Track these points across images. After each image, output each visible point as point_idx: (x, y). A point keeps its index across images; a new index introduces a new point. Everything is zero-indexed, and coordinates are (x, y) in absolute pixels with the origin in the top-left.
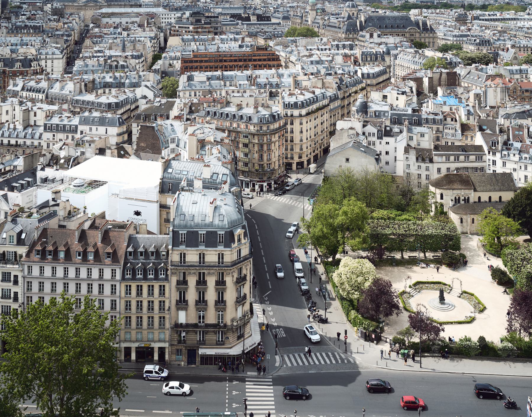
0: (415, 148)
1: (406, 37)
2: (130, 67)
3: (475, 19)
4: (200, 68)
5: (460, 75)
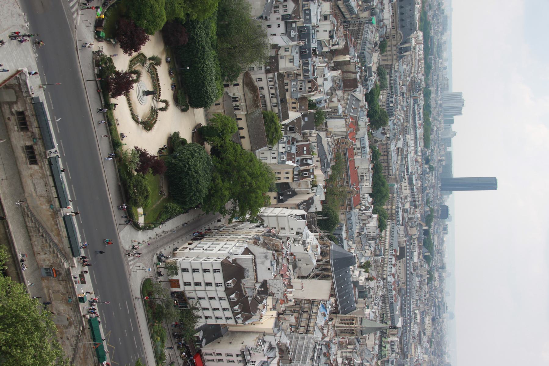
0: (278, 54)
1: (391, 31)
3: (414, 100)
5: (355, 91)
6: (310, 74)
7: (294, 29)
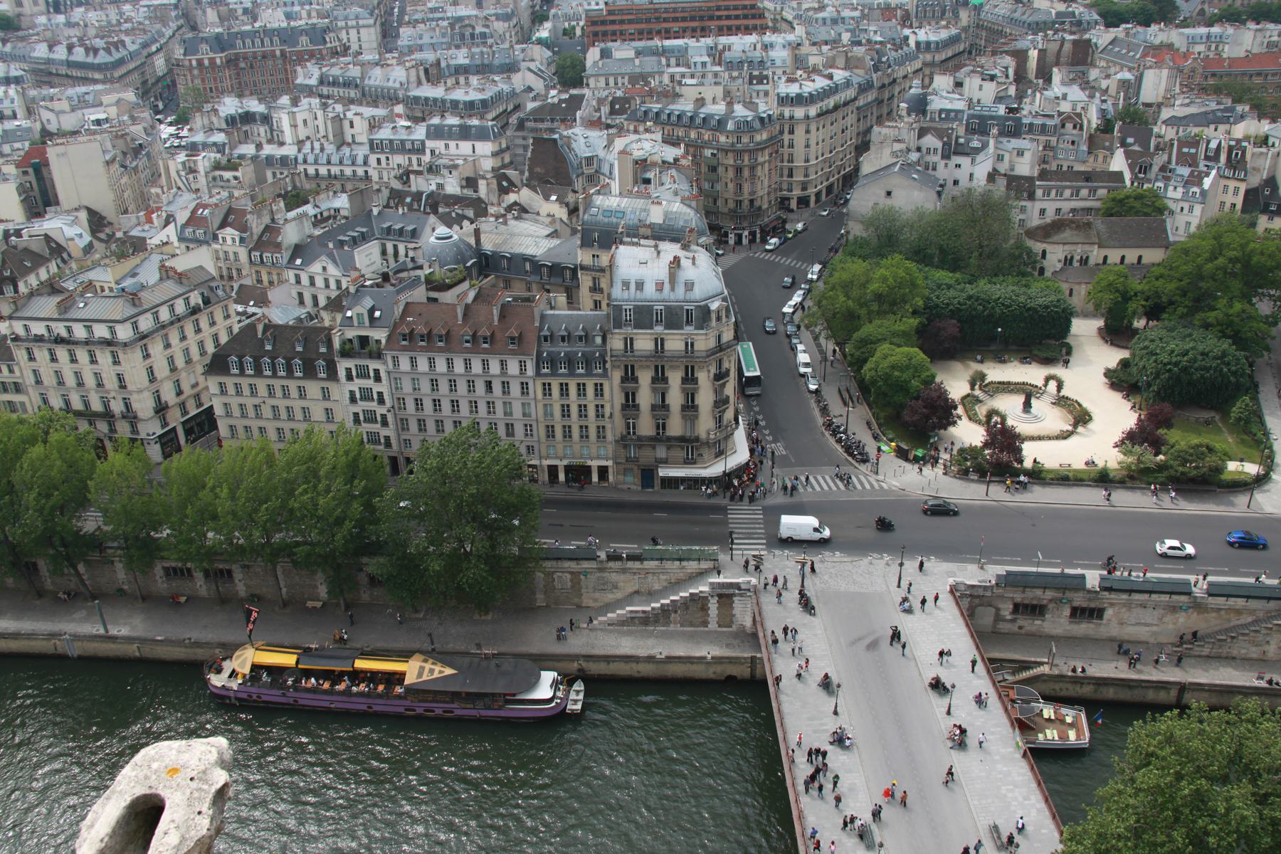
2: (496, 35)
4: (621, 34)
6: (1049, 122)
7: (968, 142)
